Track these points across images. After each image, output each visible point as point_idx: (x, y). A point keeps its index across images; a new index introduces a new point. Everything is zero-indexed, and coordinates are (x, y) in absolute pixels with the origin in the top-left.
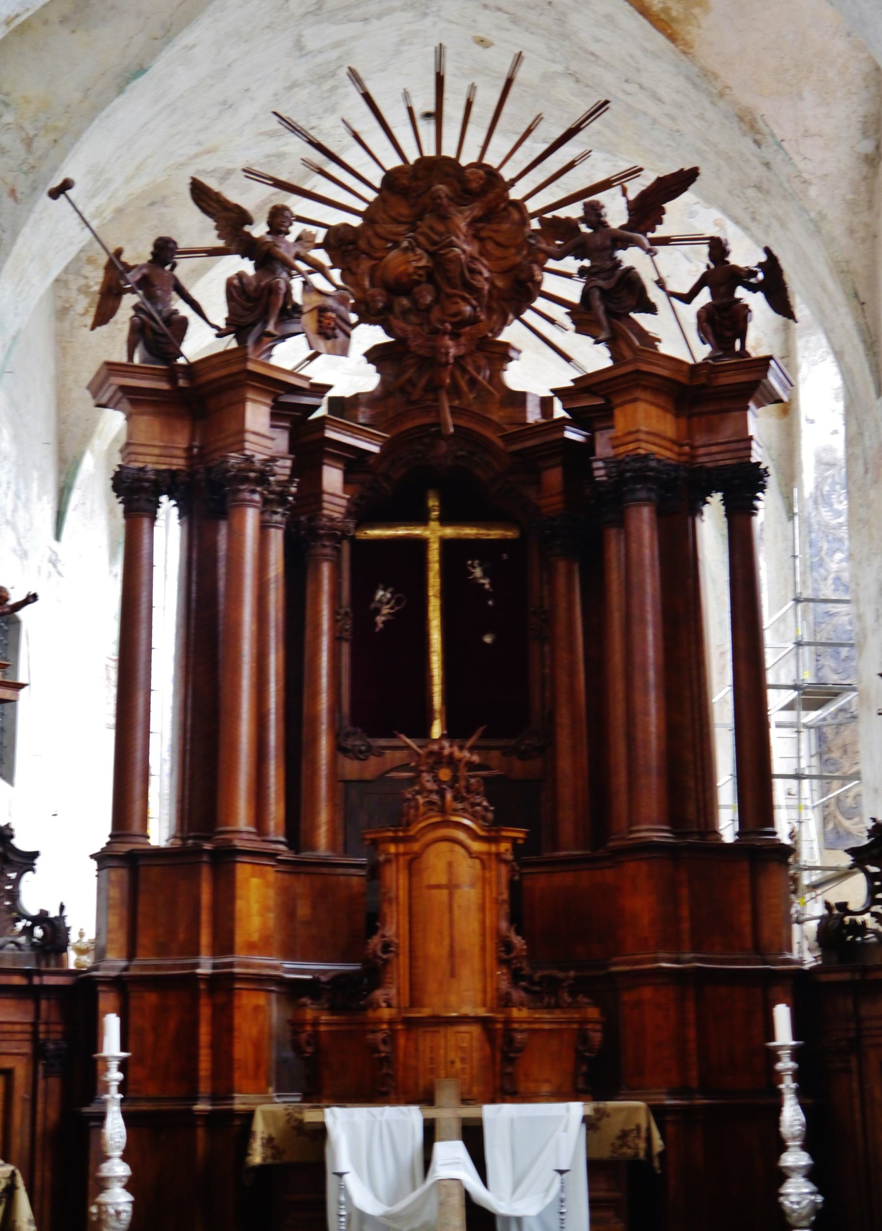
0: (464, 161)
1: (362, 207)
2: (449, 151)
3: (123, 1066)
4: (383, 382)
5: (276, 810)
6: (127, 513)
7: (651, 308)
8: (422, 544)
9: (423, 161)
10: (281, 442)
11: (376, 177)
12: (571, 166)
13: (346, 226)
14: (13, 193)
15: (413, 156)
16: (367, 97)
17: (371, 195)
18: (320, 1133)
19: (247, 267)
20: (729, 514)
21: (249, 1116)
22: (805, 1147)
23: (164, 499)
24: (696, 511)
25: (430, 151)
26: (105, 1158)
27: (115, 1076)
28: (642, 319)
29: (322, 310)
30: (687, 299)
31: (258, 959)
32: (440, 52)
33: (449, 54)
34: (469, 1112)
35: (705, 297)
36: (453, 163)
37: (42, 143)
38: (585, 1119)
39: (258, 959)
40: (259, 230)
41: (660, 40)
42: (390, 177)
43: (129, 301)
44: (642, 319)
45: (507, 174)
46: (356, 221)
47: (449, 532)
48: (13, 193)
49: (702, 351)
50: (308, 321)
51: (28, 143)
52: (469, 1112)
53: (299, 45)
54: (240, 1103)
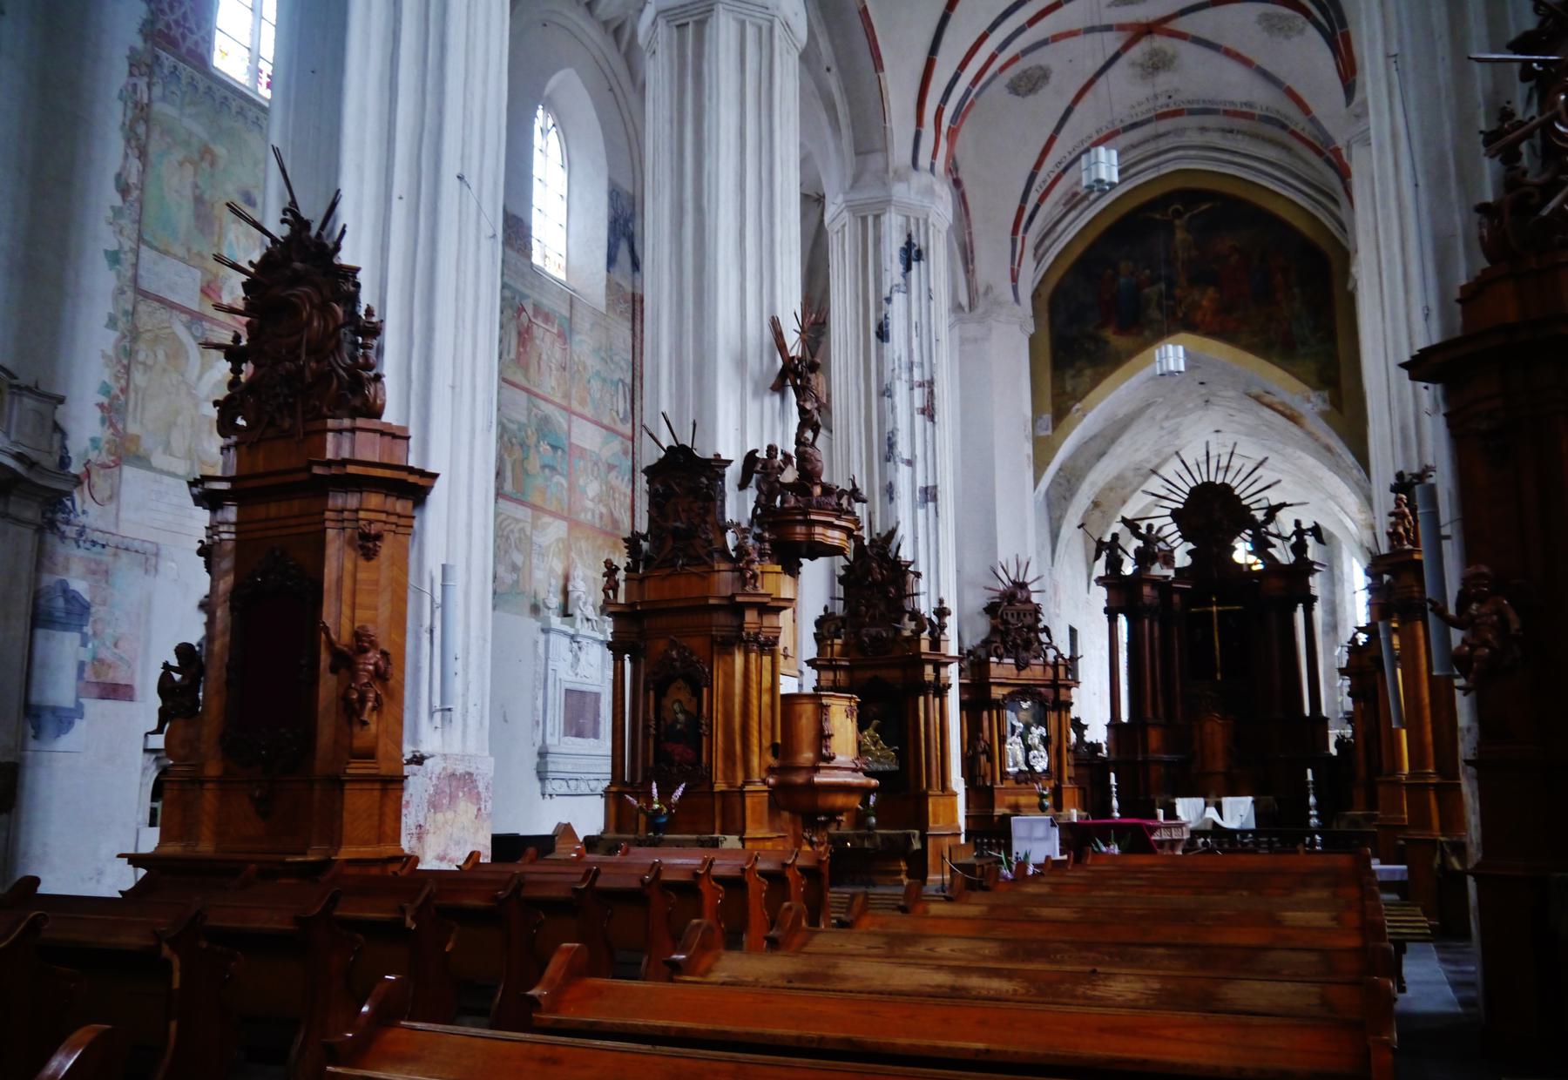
0: (1218, 482)
1: (1183, 501)
2: (1212, 479)
3: (1116, 787)
4: (1193, 562)
5: (1161, 710)
6: (1109, 621)
7: (1274, 546)
8: (1212, 612)
9: (1203, 483)
10: (1155, 593)
11: (1187, 490)
12: (1256, 481)
13: (1177, 509)
14: (1065, 498)
15: (1200, 482)
16: (1183, 462)
17: (1186, 497)
18: (1175, 804)
19: (1140, 543)
20: (1305, 611)
21: (1154, 801)
22: (1316, 809)
23: (1120, 615)
24: (1294, 609)
25: (1205, 480)
26: (1113, 811)
27: (1114, 789)
28: (1271, 550)
29: (1165, 556)
30: (1289, 539)
31: (1156, 756)
32: (1207, 443)
33: (1211, 444)
34: (1218, 800)
35: (1294, 539)
36: (1214, 483)
37: (1073, 480)
38: (1253, 802)
39: (1156, 756)
40: (1143, 531)
41: (1291, 423)
42: (1192, 489)
43: (1104, 555)
44: (1271, 550)
45: (1234, 484)
46: (1181, 506)
47: (1220, 608)
48: (1065, 498)
49: (1292, 558)
50: (1161, 560)
51: (1069, 481)
52: (1218, 800)
53: (1162, 428)
54: (1152, 797)
